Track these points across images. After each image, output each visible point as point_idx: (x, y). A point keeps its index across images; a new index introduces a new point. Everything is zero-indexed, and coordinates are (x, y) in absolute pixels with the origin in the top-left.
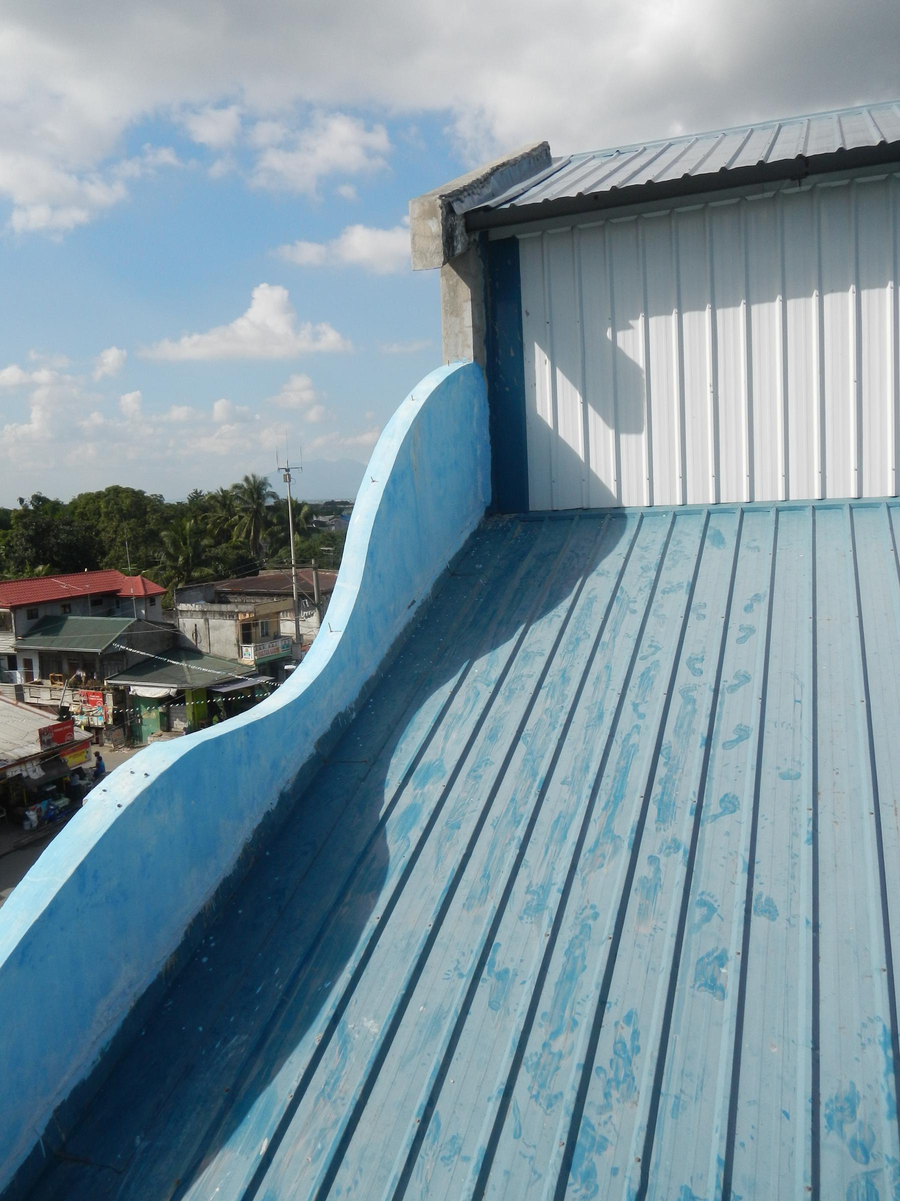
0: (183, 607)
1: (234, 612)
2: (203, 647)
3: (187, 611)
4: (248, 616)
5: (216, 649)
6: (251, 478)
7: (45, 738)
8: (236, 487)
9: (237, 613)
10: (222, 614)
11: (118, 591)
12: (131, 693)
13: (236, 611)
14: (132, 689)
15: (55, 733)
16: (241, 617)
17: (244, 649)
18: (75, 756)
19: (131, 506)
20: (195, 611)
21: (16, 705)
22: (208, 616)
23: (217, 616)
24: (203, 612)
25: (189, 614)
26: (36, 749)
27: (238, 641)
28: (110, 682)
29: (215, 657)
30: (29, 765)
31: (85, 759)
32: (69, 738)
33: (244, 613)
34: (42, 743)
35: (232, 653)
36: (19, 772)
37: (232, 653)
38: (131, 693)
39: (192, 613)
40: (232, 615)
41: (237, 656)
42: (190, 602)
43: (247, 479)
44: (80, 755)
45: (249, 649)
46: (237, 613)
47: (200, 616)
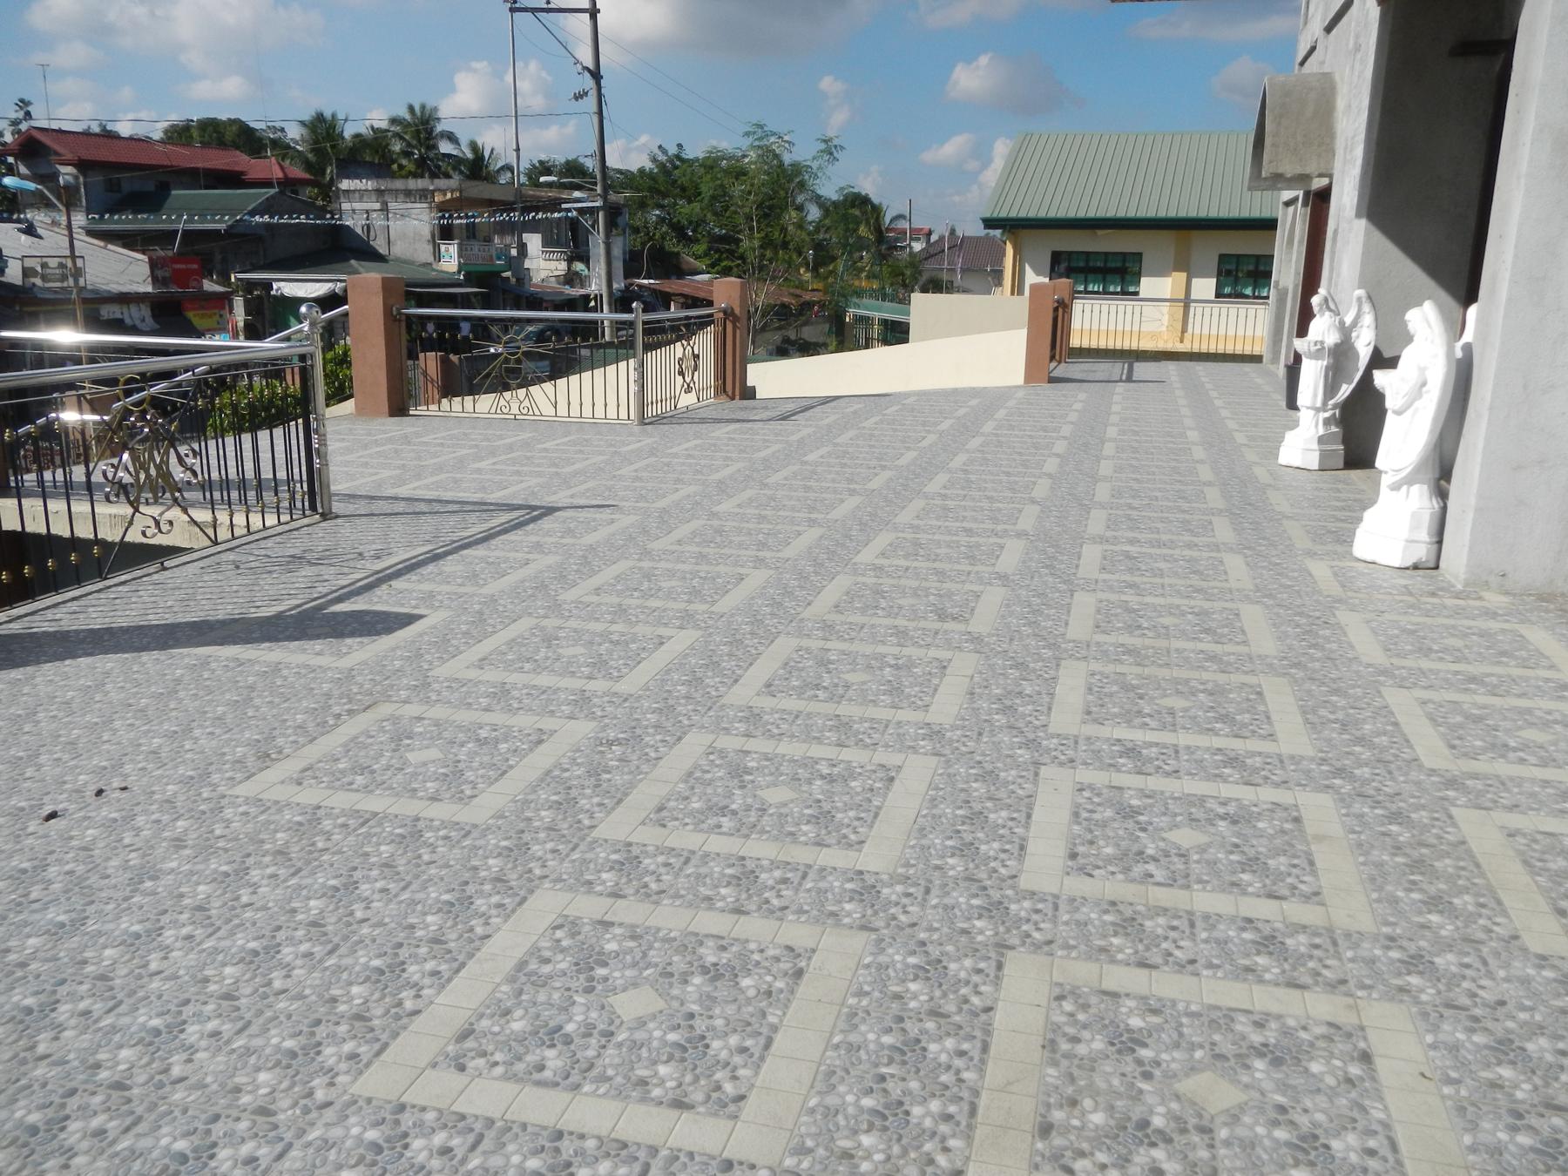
0: (345, 184)
1: (427, 190)
2: (380, 245)
3: (354, 191)
4: (449, 196)
5: (398, 250)
6: (417, 109)
7: (159, 273)
8: (394, 121)
9: (433, 192)
10: (408, 194)
11: (242, 173)
12: (273, 293)
13: (431, 188)
14: (275, 287)
15: (174, 270)
16: (438, 198)
17: (443, 248)
18: (203, 316)
19: (239, 136)
20: (366, 190)
21: (105, 248)
22: (387, 198)
23: (401, 197)
24: (379, 192)
25: (357, 195)
26: (148, 288)
27: (433, 236)
28: (240, 276)
29: (398, 260)
30: (133, 309)
31: (216, 326)
32: (194, 284)
33: (444, 192)
34: (155, 280)
35: (424, 253)
36: (119, 316)
37: (424, 253)
38: (273, 293)
39: (362, 194)
40: (424, 195)
41: (431, 259)
42: (359, 177)
43: (411, 109)
44: (210, 316)
45: (451, 248)
46: (433, 192)
47: (374, 199)
